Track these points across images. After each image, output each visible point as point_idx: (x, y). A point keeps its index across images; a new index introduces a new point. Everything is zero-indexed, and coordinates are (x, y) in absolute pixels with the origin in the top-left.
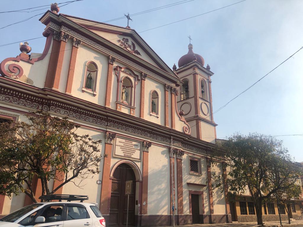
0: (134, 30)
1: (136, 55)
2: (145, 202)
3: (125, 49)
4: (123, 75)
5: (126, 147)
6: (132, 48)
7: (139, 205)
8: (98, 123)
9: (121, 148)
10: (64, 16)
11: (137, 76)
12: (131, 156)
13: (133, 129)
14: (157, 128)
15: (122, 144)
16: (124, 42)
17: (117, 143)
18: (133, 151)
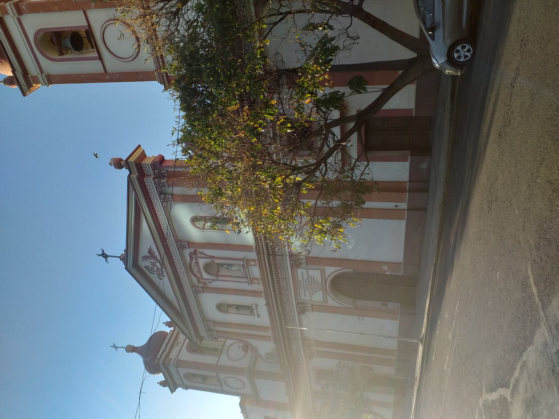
0: (126, 268)
1: (157, 254)
2: (383, 267)
3: (164, 270)
4: (205, 276)
5: (309, 288)
6: (152, 261)
7: (388, 273)
8: (292, 319)
9: (313, 295)
10: (192, 341)
11: (191, 255)
12: (319, 282)
13: (280, 281)
14: (264, 254)
15: (307, 293)
16: (155, 273)
17: (308, 298)
18: (312, 279)
